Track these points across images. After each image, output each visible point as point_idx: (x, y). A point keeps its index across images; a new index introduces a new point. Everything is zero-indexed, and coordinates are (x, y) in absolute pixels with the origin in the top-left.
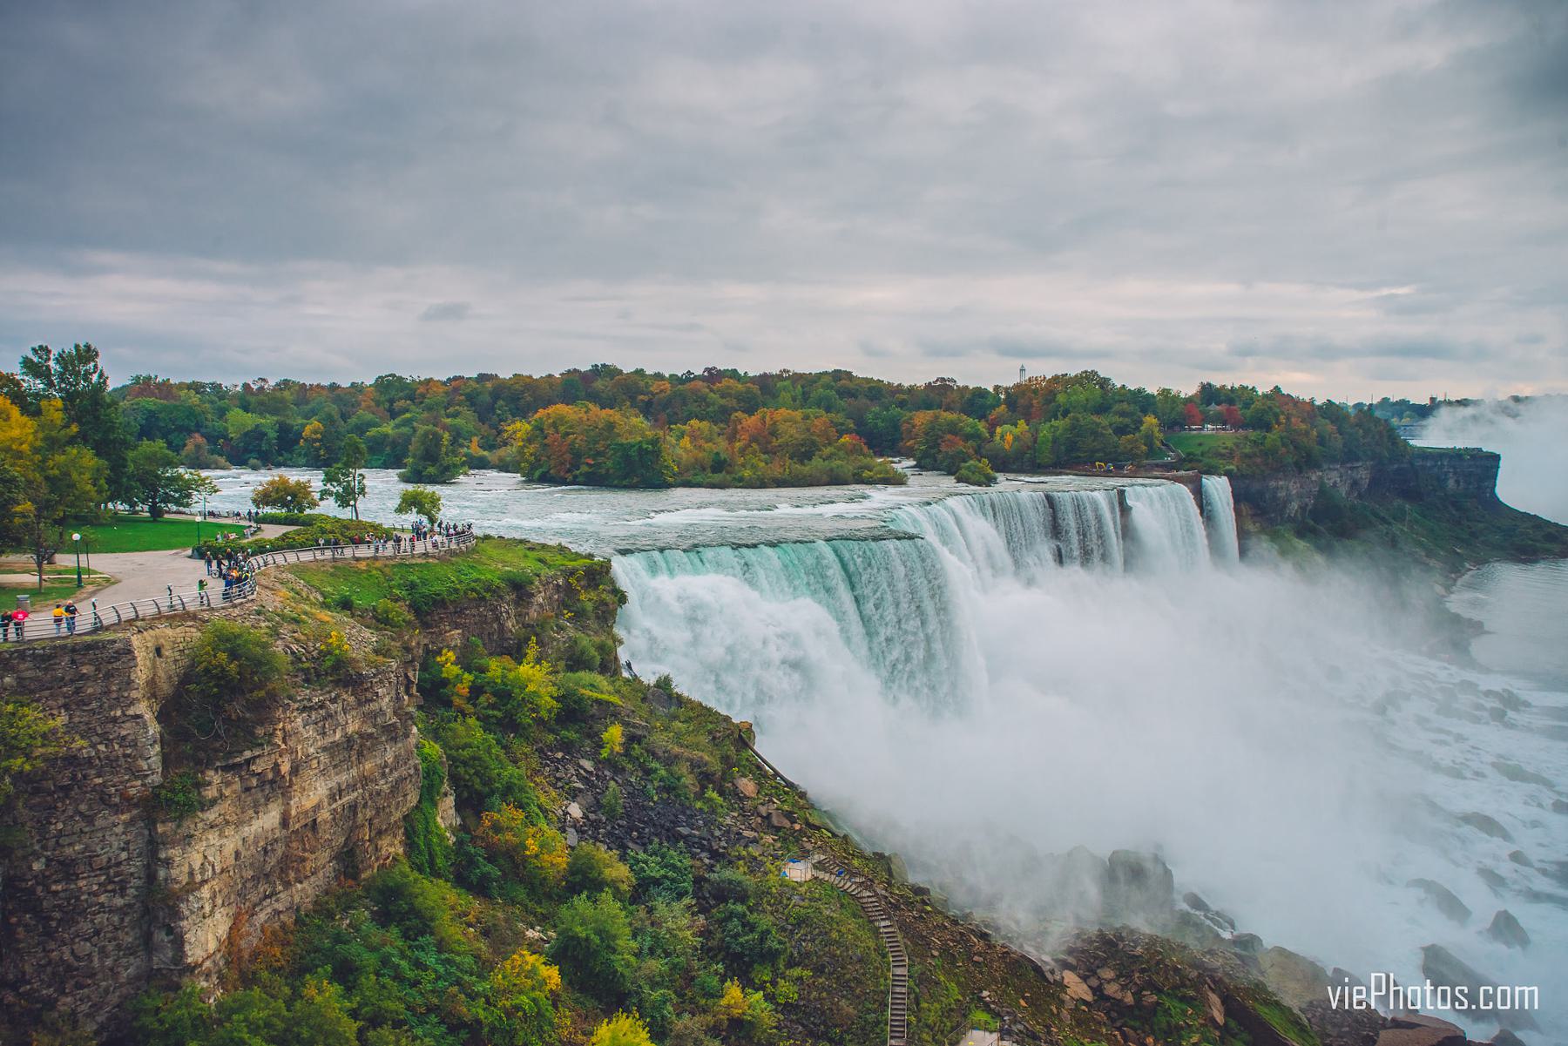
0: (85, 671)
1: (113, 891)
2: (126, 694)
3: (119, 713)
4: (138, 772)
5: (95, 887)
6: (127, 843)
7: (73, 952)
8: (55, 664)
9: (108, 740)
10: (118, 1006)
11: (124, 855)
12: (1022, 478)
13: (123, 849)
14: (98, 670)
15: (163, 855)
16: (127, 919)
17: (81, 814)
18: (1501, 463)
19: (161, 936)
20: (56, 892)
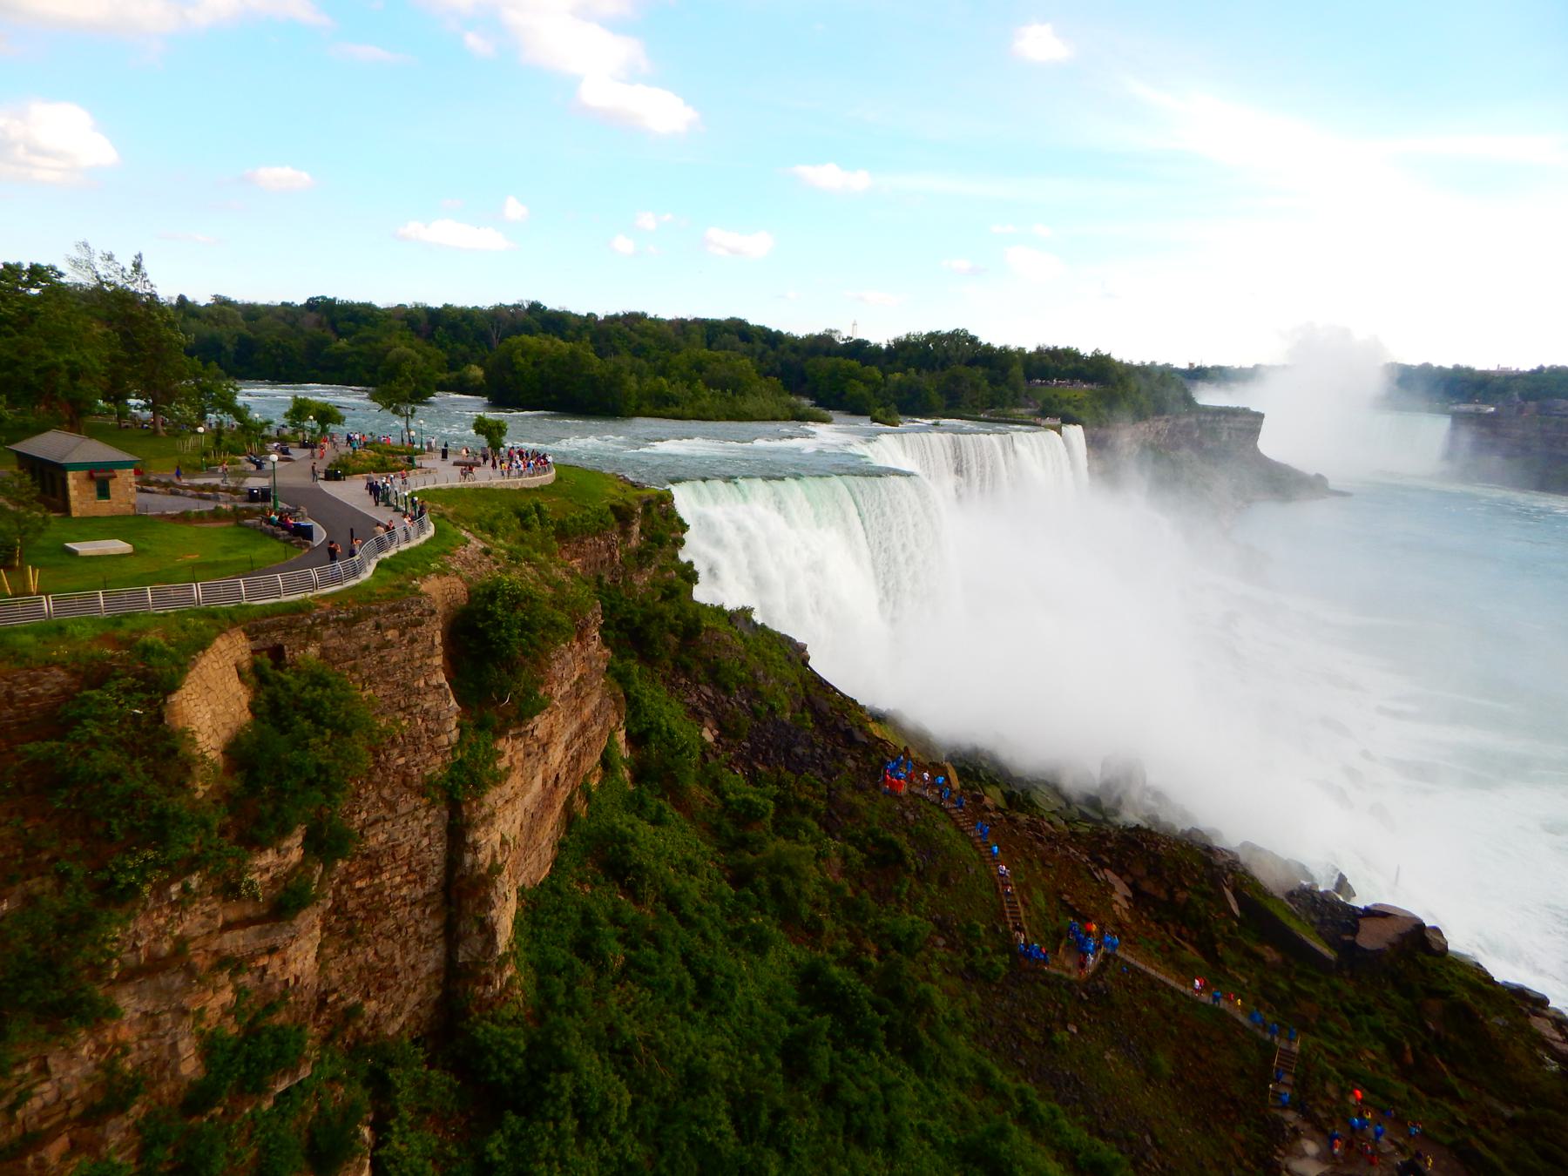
0: (389, 637)
1: (415, 882)
2: (428, 661)
3: (422, 683)
4: (439, 747)
5: (398, 879)
6: (428, 827)
7: (376, 953)
8: (360, 630)
9: (411, 714)
10: (419, 1004)
11: (425, 842)
12: (918, 420)
13: (425, 835)
14: (402, 634)
15: (470, 840)
16: (428, 911)
17: (383, 799)
18: (1265, 420)
19: (467, 926)
20: (361, 890)
